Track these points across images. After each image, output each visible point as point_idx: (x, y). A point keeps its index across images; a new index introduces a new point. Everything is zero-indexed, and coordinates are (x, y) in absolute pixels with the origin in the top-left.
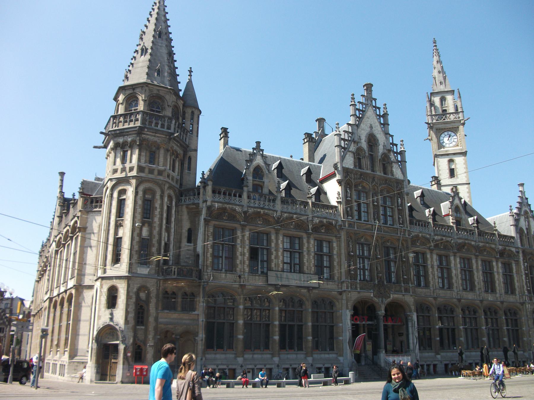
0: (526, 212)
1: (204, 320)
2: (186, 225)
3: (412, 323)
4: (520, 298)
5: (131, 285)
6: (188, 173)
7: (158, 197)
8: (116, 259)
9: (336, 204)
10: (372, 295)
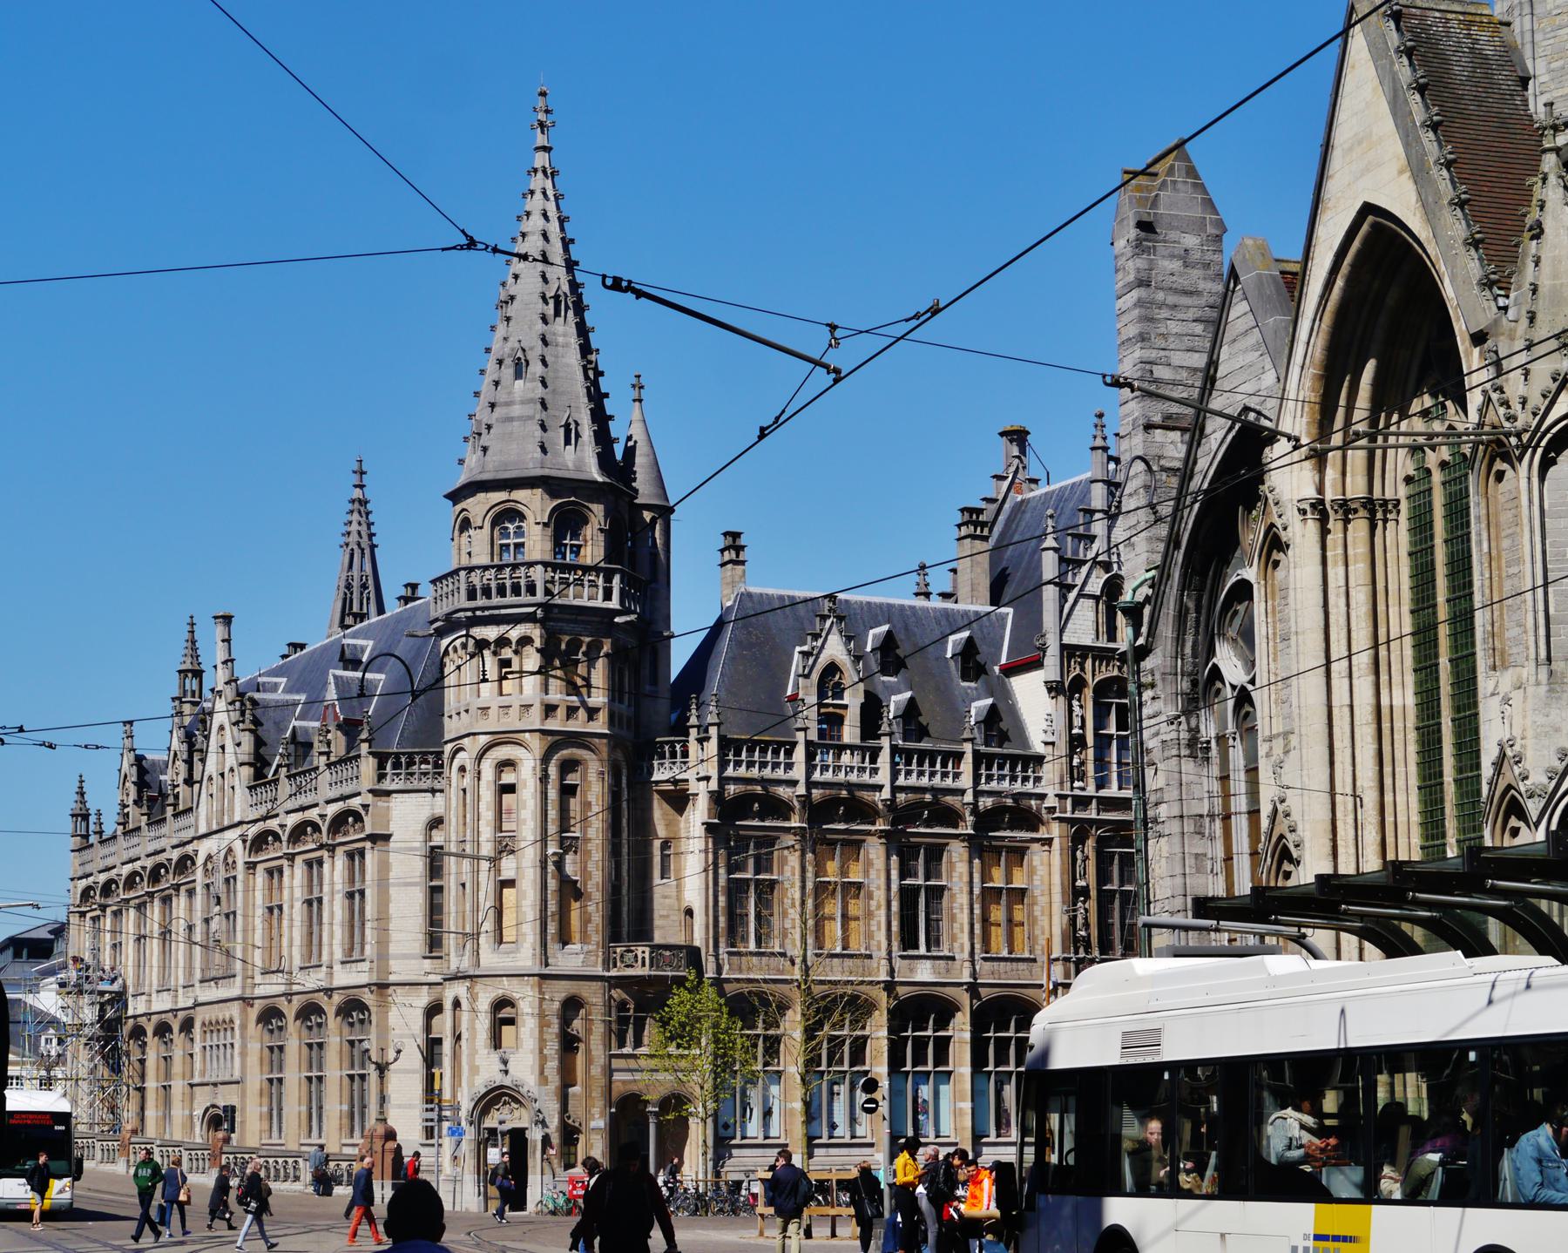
9: (1039, 748)
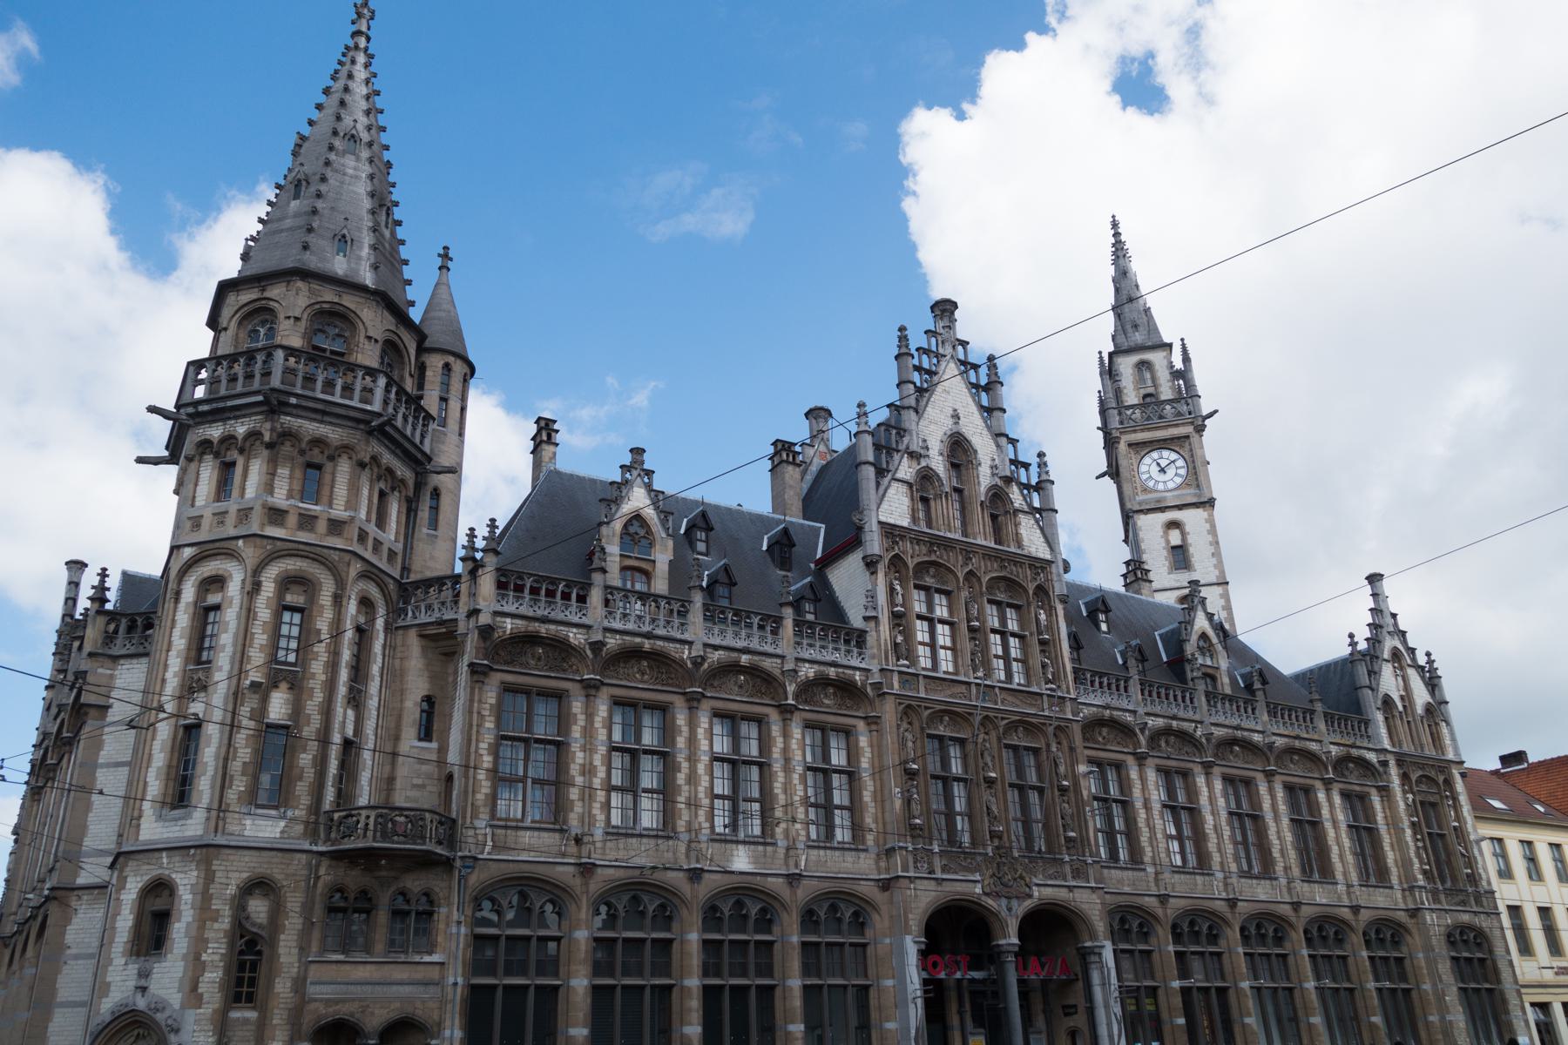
0: (1396, 655)
1: (460, 980)
2: (417, 686)
3: (1102, 973)
4: (1404, 897)
5: (218, 874)
6: (428, 535)
7: (325, 598)
8: (179, 795)
10: (978, 890)
